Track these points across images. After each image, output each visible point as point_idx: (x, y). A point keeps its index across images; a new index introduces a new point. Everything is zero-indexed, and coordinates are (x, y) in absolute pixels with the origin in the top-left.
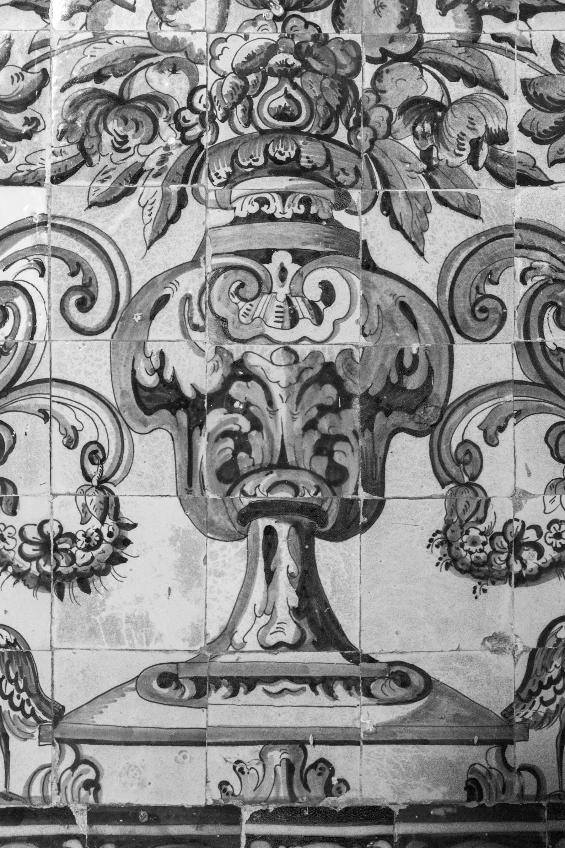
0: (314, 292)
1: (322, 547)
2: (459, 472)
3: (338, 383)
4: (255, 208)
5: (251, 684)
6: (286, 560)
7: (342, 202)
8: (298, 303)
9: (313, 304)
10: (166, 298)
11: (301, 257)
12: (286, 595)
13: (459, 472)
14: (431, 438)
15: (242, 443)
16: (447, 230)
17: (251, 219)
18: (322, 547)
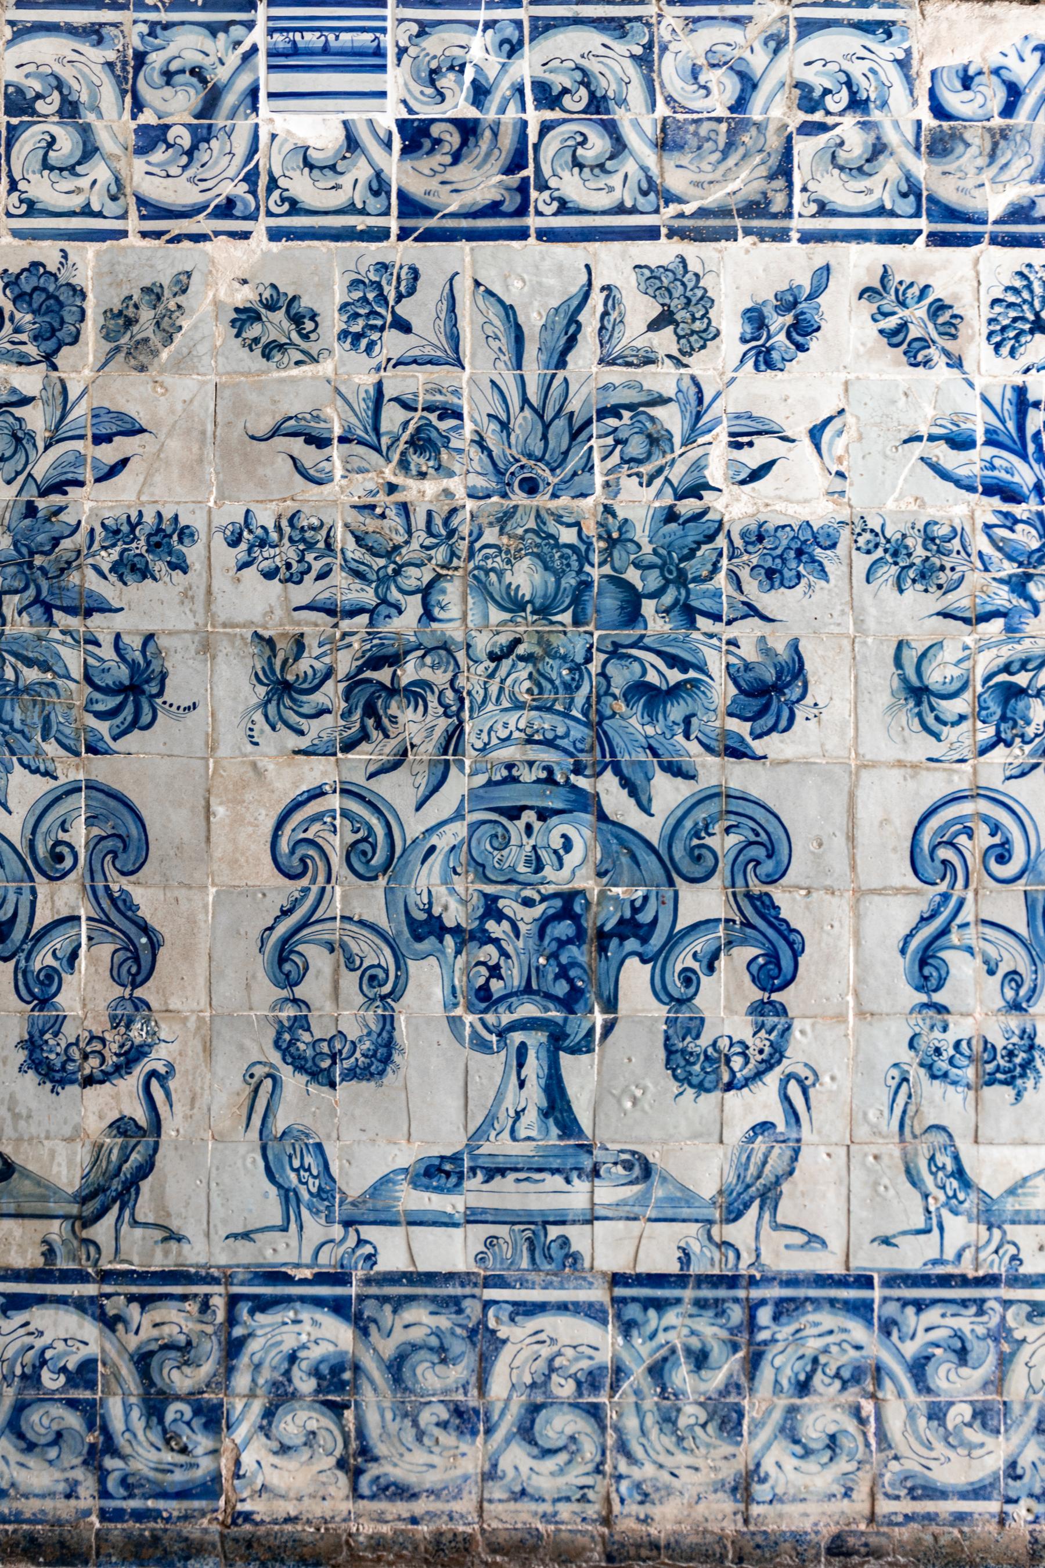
0: (557, 843)
1: (565, 1058)
2: (678, 997)
3: (576, 918)
4: (505, 773)
5: (502, 1172)
6: (533, 1067)
7: (578, 769)
8: (543, 854)
9: (555, 852)
10: (432, 849)
11: (543, 815)
12: (534, 1095)
13: (678, 997)
14: (654, 968)
15: (495, 971)
16: (668, 793)
17: (504, 781)
18: (565, 1058)
